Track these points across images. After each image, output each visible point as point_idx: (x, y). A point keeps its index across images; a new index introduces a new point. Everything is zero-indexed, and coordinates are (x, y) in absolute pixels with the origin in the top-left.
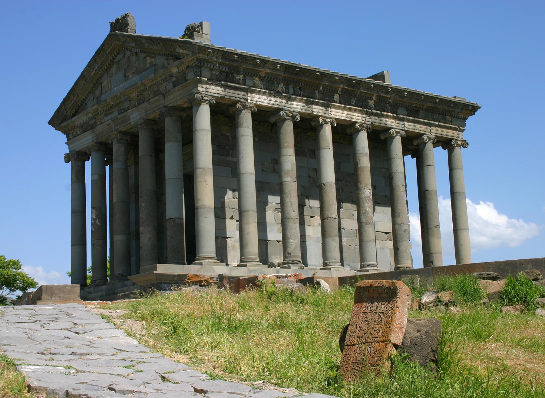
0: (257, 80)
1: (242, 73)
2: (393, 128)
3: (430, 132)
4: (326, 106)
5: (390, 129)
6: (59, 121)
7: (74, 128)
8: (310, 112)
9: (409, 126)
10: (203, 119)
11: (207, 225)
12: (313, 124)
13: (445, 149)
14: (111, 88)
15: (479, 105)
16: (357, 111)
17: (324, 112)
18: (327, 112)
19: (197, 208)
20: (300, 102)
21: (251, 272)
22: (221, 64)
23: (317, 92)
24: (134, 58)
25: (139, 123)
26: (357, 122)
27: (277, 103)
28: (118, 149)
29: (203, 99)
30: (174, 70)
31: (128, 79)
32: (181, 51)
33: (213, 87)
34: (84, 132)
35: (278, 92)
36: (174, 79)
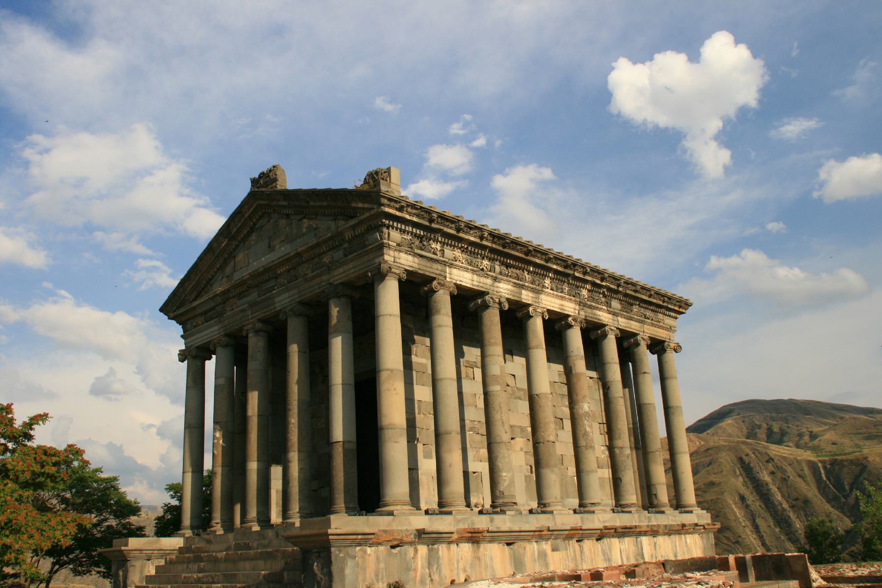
0: (458, 253)
4: (537, 292)
5: (604, 326)
6: (176, 307)
7: (196, 316)
9: (623, 323)
10: (389, 299)
11: (395, 452)
12: (519, 315)
13: (653, 354)
14: (249, 263)
15: (691, 301)
19: (382, 429)
21: (459, 521)
23: (526, 273)
24: (283, 222)
25: (289, 308)
26: (568, 316)
28: (256, 345)
30: (348, 235)
31: (274, 250)
32: (360, 205)
33: (402, 255)
34: (207, 322)
35: (482, 270)
36: (346, 245)
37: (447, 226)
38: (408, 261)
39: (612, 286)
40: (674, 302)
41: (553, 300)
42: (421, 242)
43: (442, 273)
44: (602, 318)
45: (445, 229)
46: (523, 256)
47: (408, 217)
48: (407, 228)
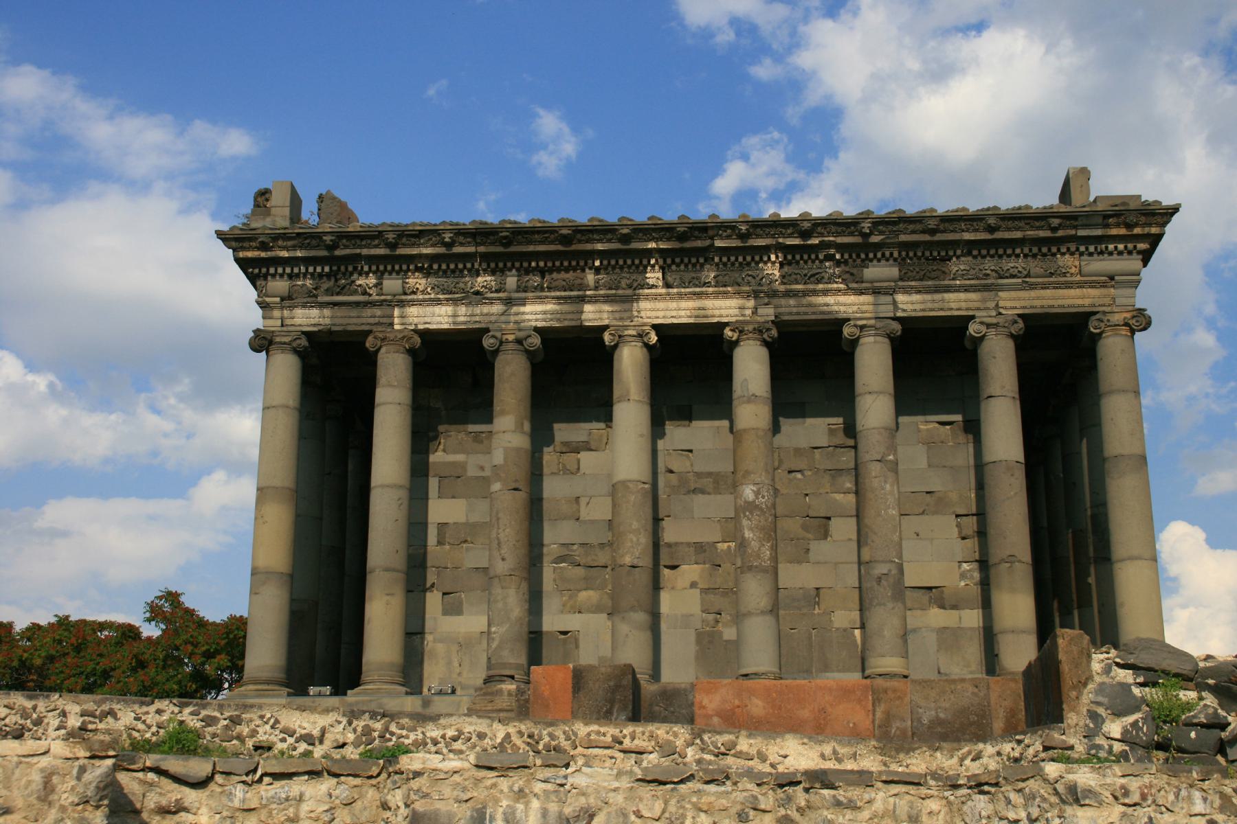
1: (366, 268)
2: (849, 320)
3: (997, 305)
8: (573, 323)
9: (911, 303)
15: (1167, 202)
16: (725, 295)
17: (617, 315)
18: (626, 315)
20: (542, 303)
22: (307, 261)
26: (727, 324)
27: (477, 319)
29: (271, 342)
33: (299, 312)
35: (477, 293)
37: (368, 246)
38: (307, 318)
39: (840, 240)
40: (1100, 221)
41: (673, 305)
42: (336, 280)
43: (382, 320)
44: (836, 308)
45: (365, 252)
46: (560, 248)
47: (285, 254)
48: (296, 270)
